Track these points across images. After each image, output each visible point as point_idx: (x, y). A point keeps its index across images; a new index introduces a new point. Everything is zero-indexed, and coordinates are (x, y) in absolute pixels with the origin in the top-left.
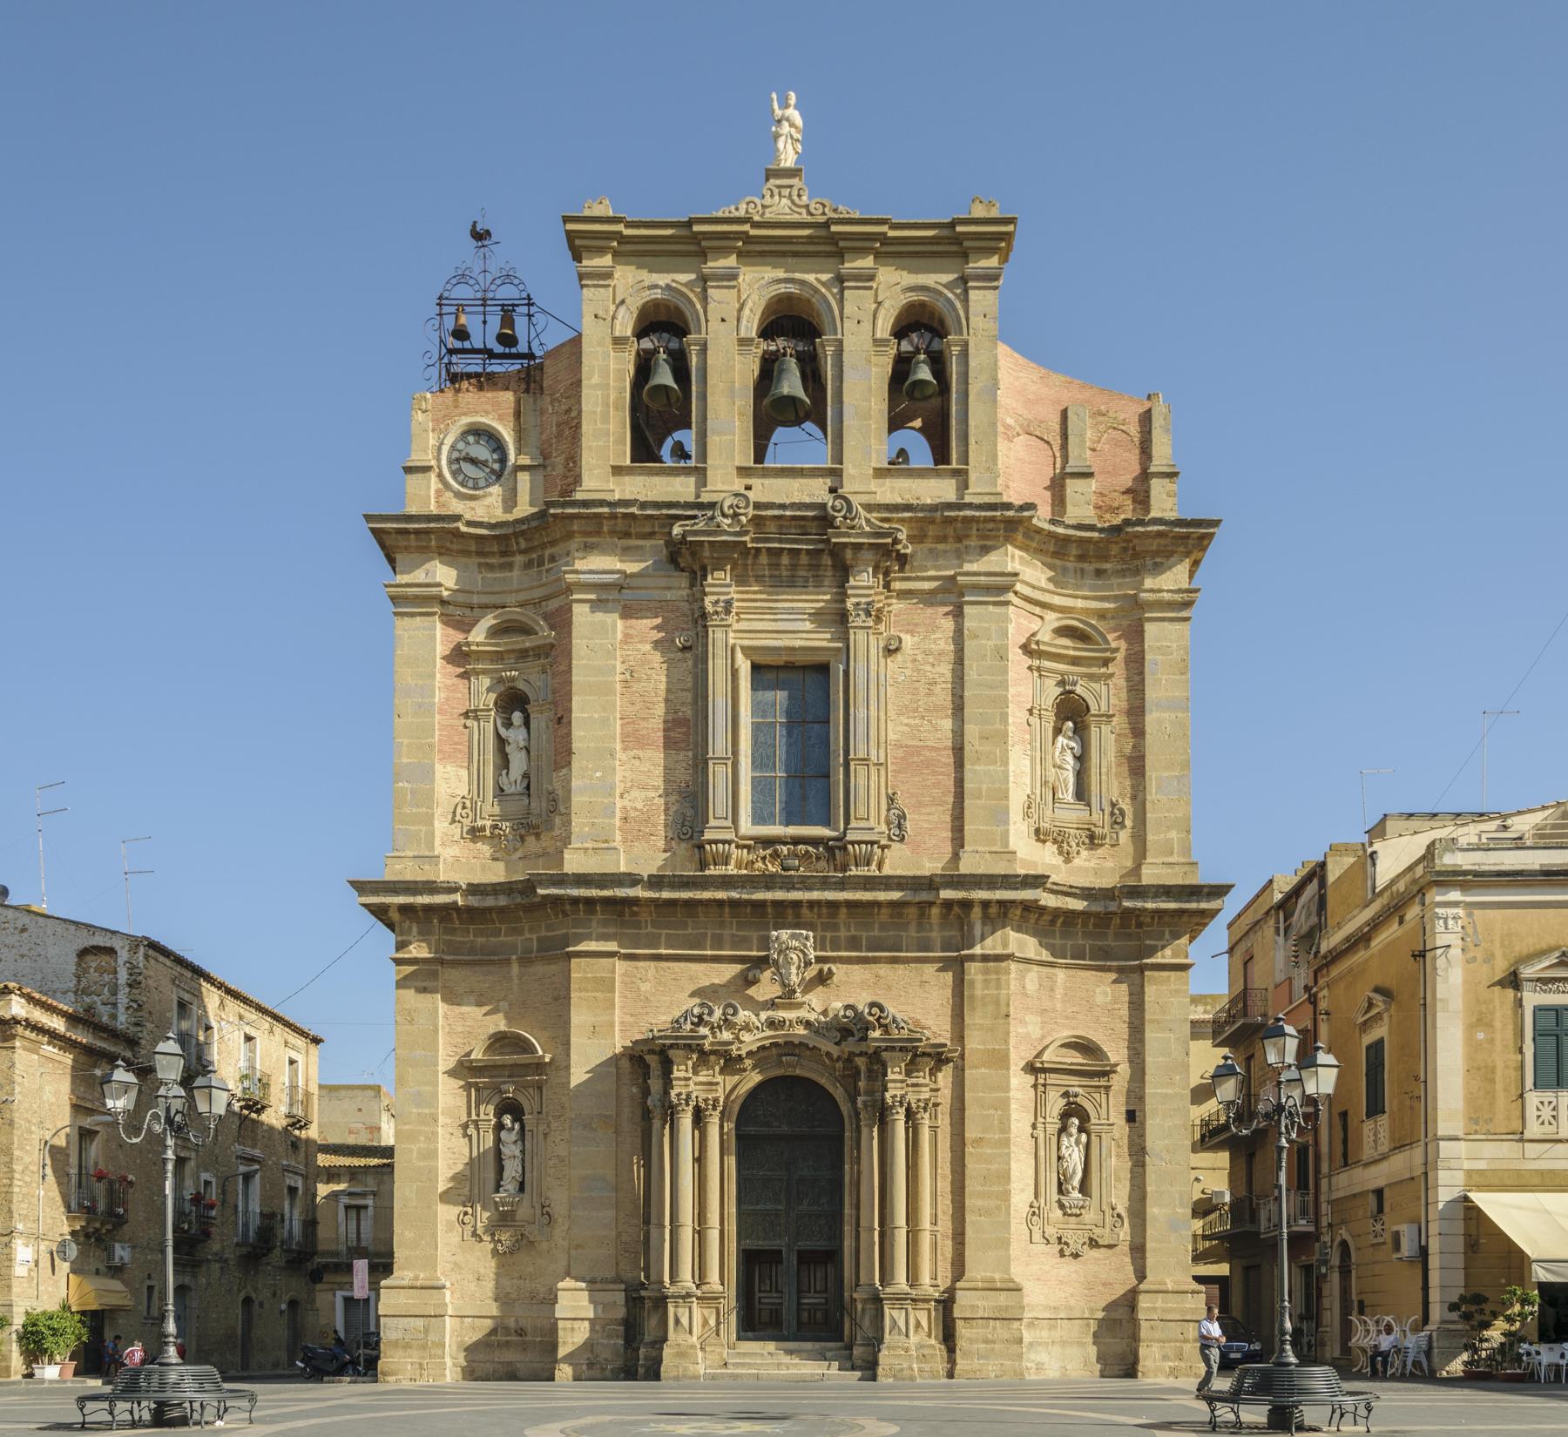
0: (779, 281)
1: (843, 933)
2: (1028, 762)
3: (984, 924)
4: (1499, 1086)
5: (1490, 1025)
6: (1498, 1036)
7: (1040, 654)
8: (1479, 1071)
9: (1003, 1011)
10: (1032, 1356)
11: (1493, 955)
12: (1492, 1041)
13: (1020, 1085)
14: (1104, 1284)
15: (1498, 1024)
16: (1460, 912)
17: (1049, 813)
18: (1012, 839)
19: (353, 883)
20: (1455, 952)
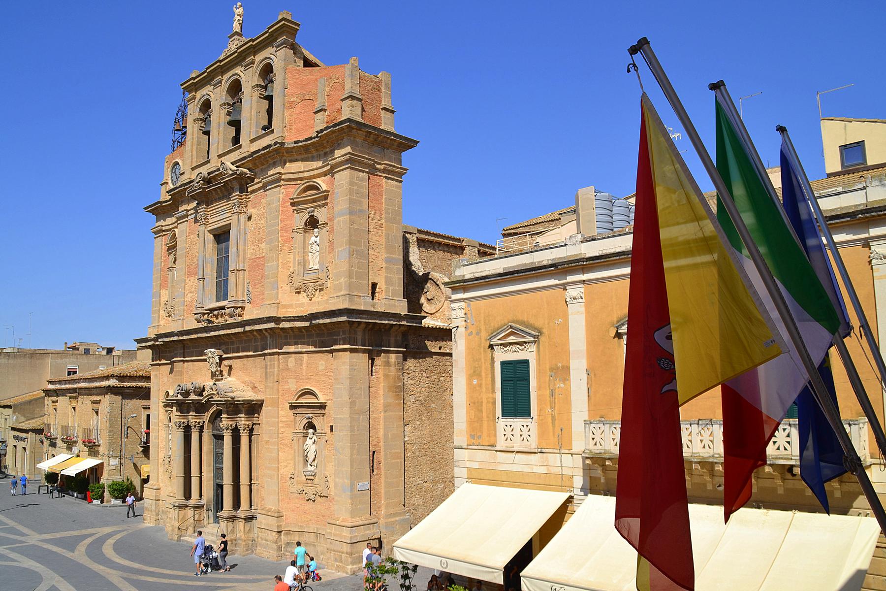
2: (292, 256)
4: (484, 414)
5: (479, 375)
6: (484, 382)
7: (298, 203)
8: (475, 404)
9: (276, 379)
10: (289, 549)
11: (480, 330)
12: (480, 385)
13: (285, 413)
15: (483, 374)
16: (462, 304)
17: (301, 278)
20: (462, 330)
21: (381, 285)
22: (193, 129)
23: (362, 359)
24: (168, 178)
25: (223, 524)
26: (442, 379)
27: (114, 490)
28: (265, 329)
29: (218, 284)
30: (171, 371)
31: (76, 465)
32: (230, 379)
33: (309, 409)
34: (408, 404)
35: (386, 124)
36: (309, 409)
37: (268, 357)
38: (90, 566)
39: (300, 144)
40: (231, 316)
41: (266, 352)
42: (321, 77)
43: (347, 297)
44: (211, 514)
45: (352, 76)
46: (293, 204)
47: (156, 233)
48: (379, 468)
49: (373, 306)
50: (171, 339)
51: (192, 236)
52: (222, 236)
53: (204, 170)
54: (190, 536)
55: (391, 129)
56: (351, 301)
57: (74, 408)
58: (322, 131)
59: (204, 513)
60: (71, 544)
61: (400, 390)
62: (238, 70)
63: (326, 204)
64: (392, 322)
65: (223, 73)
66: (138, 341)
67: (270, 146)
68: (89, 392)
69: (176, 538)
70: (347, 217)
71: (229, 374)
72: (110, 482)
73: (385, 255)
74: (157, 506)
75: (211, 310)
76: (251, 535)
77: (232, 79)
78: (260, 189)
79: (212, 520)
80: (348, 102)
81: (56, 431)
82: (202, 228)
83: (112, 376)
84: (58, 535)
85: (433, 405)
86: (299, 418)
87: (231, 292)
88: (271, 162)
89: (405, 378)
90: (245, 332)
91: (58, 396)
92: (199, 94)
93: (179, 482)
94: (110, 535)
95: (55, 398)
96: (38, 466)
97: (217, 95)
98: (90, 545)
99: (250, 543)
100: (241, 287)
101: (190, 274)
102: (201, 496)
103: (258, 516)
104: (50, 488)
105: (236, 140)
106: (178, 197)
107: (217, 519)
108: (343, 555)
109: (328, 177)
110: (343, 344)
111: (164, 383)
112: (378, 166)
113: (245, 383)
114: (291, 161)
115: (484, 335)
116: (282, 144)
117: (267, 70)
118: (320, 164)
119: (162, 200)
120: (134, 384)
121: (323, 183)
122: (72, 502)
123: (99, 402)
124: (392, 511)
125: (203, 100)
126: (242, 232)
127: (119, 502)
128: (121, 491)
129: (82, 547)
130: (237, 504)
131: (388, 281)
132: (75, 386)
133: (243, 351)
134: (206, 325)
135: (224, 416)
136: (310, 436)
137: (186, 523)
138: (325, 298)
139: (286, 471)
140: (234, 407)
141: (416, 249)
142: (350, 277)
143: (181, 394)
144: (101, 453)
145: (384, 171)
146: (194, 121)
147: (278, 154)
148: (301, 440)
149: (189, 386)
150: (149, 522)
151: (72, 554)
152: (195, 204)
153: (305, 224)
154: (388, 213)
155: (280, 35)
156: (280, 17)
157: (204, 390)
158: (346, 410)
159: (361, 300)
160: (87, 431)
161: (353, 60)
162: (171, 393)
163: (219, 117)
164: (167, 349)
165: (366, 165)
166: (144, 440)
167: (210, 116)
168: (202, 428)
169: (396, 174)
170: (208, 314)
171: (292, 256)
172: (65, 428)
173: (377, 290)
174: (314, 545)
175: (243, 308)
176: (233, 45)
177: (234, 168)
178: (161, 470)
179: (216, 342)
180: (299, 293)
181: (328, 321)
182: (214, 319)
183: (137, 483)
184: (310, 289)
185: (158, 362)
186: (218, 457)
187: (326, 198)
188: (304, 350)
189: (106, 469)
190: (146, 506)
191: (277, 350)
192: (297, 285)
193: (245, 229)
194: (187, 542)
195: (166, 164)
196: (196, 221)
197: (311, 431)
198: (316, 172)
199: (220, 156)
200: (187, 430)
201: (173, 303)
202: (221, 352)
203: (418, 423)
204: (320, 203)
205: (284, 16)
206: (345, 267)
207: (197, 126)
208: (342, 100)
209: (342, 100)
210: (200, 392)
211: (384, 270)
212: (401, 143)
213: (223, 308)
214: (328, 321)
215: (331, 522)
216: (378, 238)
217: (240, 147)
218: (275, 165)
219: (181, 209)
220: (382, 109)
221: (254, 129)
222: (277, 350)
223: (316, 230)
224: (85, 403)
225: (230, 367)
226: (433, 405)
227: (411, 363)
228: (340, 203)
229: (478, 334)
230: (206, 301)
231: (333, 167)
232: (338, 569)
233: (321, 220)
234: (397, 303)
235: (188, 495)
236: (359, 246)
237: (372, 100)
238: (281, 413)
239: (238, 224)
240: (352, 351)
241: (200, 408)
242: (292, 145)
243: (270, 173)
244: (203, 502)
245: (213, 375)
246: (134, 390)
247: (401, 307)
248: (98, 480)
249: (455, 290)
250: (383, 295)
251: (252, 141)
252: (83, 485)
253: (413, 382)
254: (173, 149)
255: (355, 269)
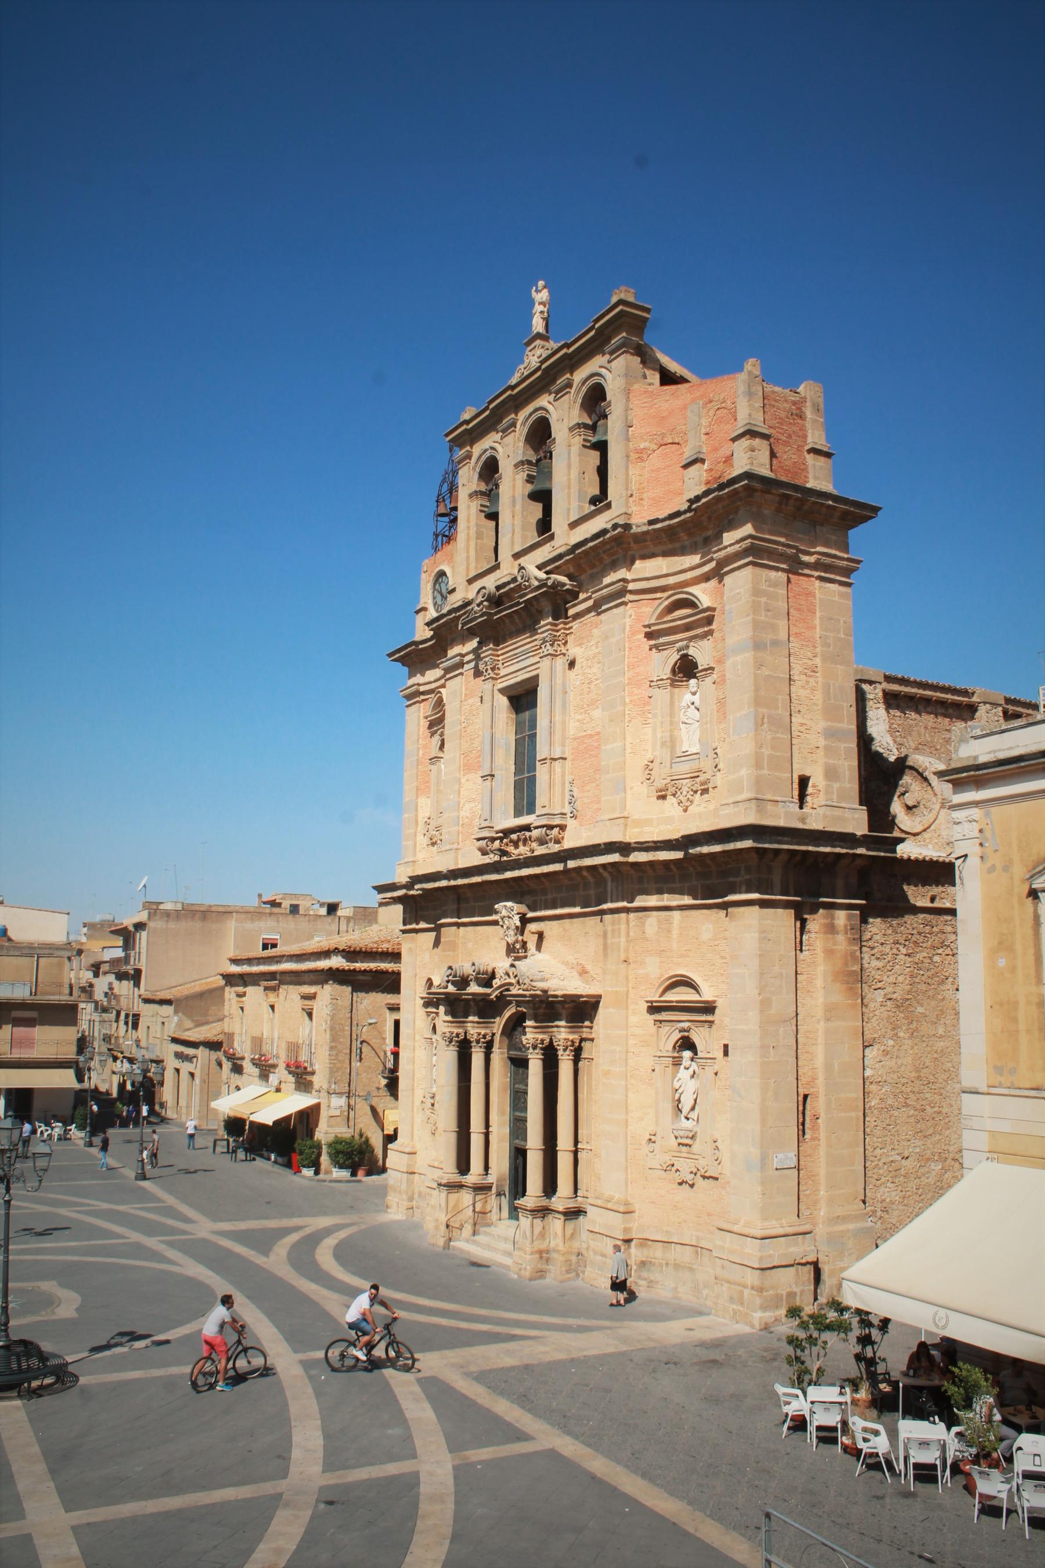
0: (531, 415)
1: (550, 897)
2: (649, 730)
3: (612, 881)
4: (1022, 1026)
5: (1010, 949)
9: (623, 958)
10: (644, 1274)
11: (1011, 861)
12: (1013, 970)
14: (709, 1215)
15: (1019, 948)
16: (975, 813)
18: (629, 803)
19: (375, 888)
21: (817, 781)
22: (468, 511)
23: (785, 918)
24: (427, 598)
25: (525, 1221)
26: (936, 958)
27: (338, 1152)
28: (604, 866)
29: (518, 786)
30: (437, 943)
31: (271, 1105)
32: (539, 956)
33: (683, 1013)
34: (872, 1005)
35: (818, 477)
36: (683, 1013)
37: (607, 918)
38: (294, 1283)
39: (659, 526)
40: (542, 842)
41: (605, 906)
42: (694, 401)
43: (753, 804)
44: (505, 1202)
45: (750, 394)
46: (649, 636)
47: (408, 697)
48: (815, 1128)
49: (803, 820)
50: (437, 884)
51: (471, 701)
52: (523, 698)
53: (490, 583)
54: (467, 1241)
55: (827, 487)
56: (760, 810)
57: (272, 1007)
58: (698, 498)
59: (493, 1201)
60: (263, 1242)
61: (855, 979)
62: (544, 401)
63: (711, 633)
64: (838, 850)
65: (517, 409)
66: (381, 889)
67: (604, 532)
68: (296, 978)
69: (441, 1242)
70: (749, 655)
71: (539, 947)
72: (331, 1138)
73: (822, 724)
74: (410, 1183)
75: (507, 832)
76: (576, 1244)
77: (534, 417)
78: (588, 611)
79: (505, 1213)
80: (745, 442)
81: (242, 1047)
82: (488, 685)
83: (336, 951)
84: (243, 1226)
85: (920, 1009)
86: (666, 1029)
87: (541, 799)
88: (607, 560)
89: (866, 956)
90: (566, 871)
91: (245, 985)
92: (477, 449)
93: (448, 1141)
94: (328, 1232)
95: (240, 989)
96: (214, 1104)
97: (509, 447)
98: (295, 1246)
99: (574, 1258)
100: (558, 789)
101: (468, 768)
102: (487, 1168)
103: (590, 1210)
104: (232, 1144)
105: (544, 526)
106: (446, 632)
107: (514, 1212)
108: (746, 1292)
109: (713, 583)
110: (748, 891)
111: (425, 962)
112: (805, 558)
113: (566, 964)
114: (644, 557)
115: (1019, 871)
116: (627, 527)
117: (595, 399)
118: (696, 559)
119: (418, 638)
120: (373, 966)
121: (703, 595)
122: (265, 1171)
123: (312, 997)
124: (839, 1211)
125: (484, 458)
126: (558, 688)
127: (345, 1174)
128: (349, 1155)
129: (282, 1249)
130: (550, 1186)
131: (831, 774)
132: (273, 968)
133: (562, 906)
134: (497, 858)
135: (528, 1023)
136: (686, 1062)
137: (460, 1217)
138: (712, 807)
139: (641, 1128)
140: (548, 1008)
141: (882, 712)
142: (758, 765)
143: (454, 983)
144: (316, 1086)
145: (816, 566)
146: (471, 496)
147: (621, 546)
148: (670, 1070)
149: (468, 970)
150: (395, 1212)
151: (265, 1259)
152: (474, 643)
153: (673, 671)
154: (826, 645)
155: (616, 332)
156: (614, 299)
157: (493, 975)
158: (753, 1016)
159: (780, 809)
160: (294, 1048)
161: (752, 366)
162: (436, 982)
163: (513, 485)
164: (432, 903)
165: (782, 557)
166: (390, 1065)
167: (497, 486)
168: (489, 1047)
169: (840, 572)
170: (501, 839)
171: (649, 730)
172: (257, 1042)
173: (810, 790)
174: (691, 1269)
175: (562, 828)
176: (533, 358)
177: (542, 575)
178: (419, 1118)
179: (516, 890)
180: (664, 797)
181: (717, 848)
182: (510, 849)
183: (376, 1141)
184: (685, 790)
185: (414, 926)
186: (518, 1099)
187: (709, 621)
188: (674, 903)
189: (324, 1114)
190: (391, 1182)
191: (625, 904)
192: (660, 783)
193: (564, 684)
194: (461, 1251)
195: (423, 576)
196: (478, 673)
197: (687, 1054)
198: (689, 575)
199: (517, 556)
200: (464, 1050)
201: (440, 822)
202: (523, 908)
203: (891, 1042)
204: (699, 631)
205: (622, 296)
206: (746, 746)
207: (475, 505)
208: (734, 440)
209: (734, 440)
210: (487, 979)
211: (821, 752)
212: (845, 514)
213: (527, 828)
214: (717, 848)
215: (725, 1226)
216: (809, 693)
217: (552, 537)
218: (614, 566)
219: (451, 653)
220: (810, 451)
221: (575, 504)
222: (625, 904)
223: (693, 681)
224: (290, 996)
225: (541, 936)
226: (920, 1009)
227: (876, 926)
228: (735, 628)
229: (1006, 869)
230: (497, 815)
231: (721, 564)
232: (735, 1317)
233: (702, 662)
234: (847, 814)
235: (463, 1165)
236: (775, 712)
237: (790, 436)
238: (633, 1019)
239: (551, 676)
240: (763, 904)
241: (487, 1008)
242: (645, 528)
243: (607, 580)
244: (492, 1179)
245: (510, 950)
246: (372, 975)
247: (856, 821)
248: (310, 1133)
249: (958, 785)
250: (821, 800)
251: (573, 525)
252: (285, 1142)
253: (880, 964)
254: (436, 550)
255: (766, 751)
